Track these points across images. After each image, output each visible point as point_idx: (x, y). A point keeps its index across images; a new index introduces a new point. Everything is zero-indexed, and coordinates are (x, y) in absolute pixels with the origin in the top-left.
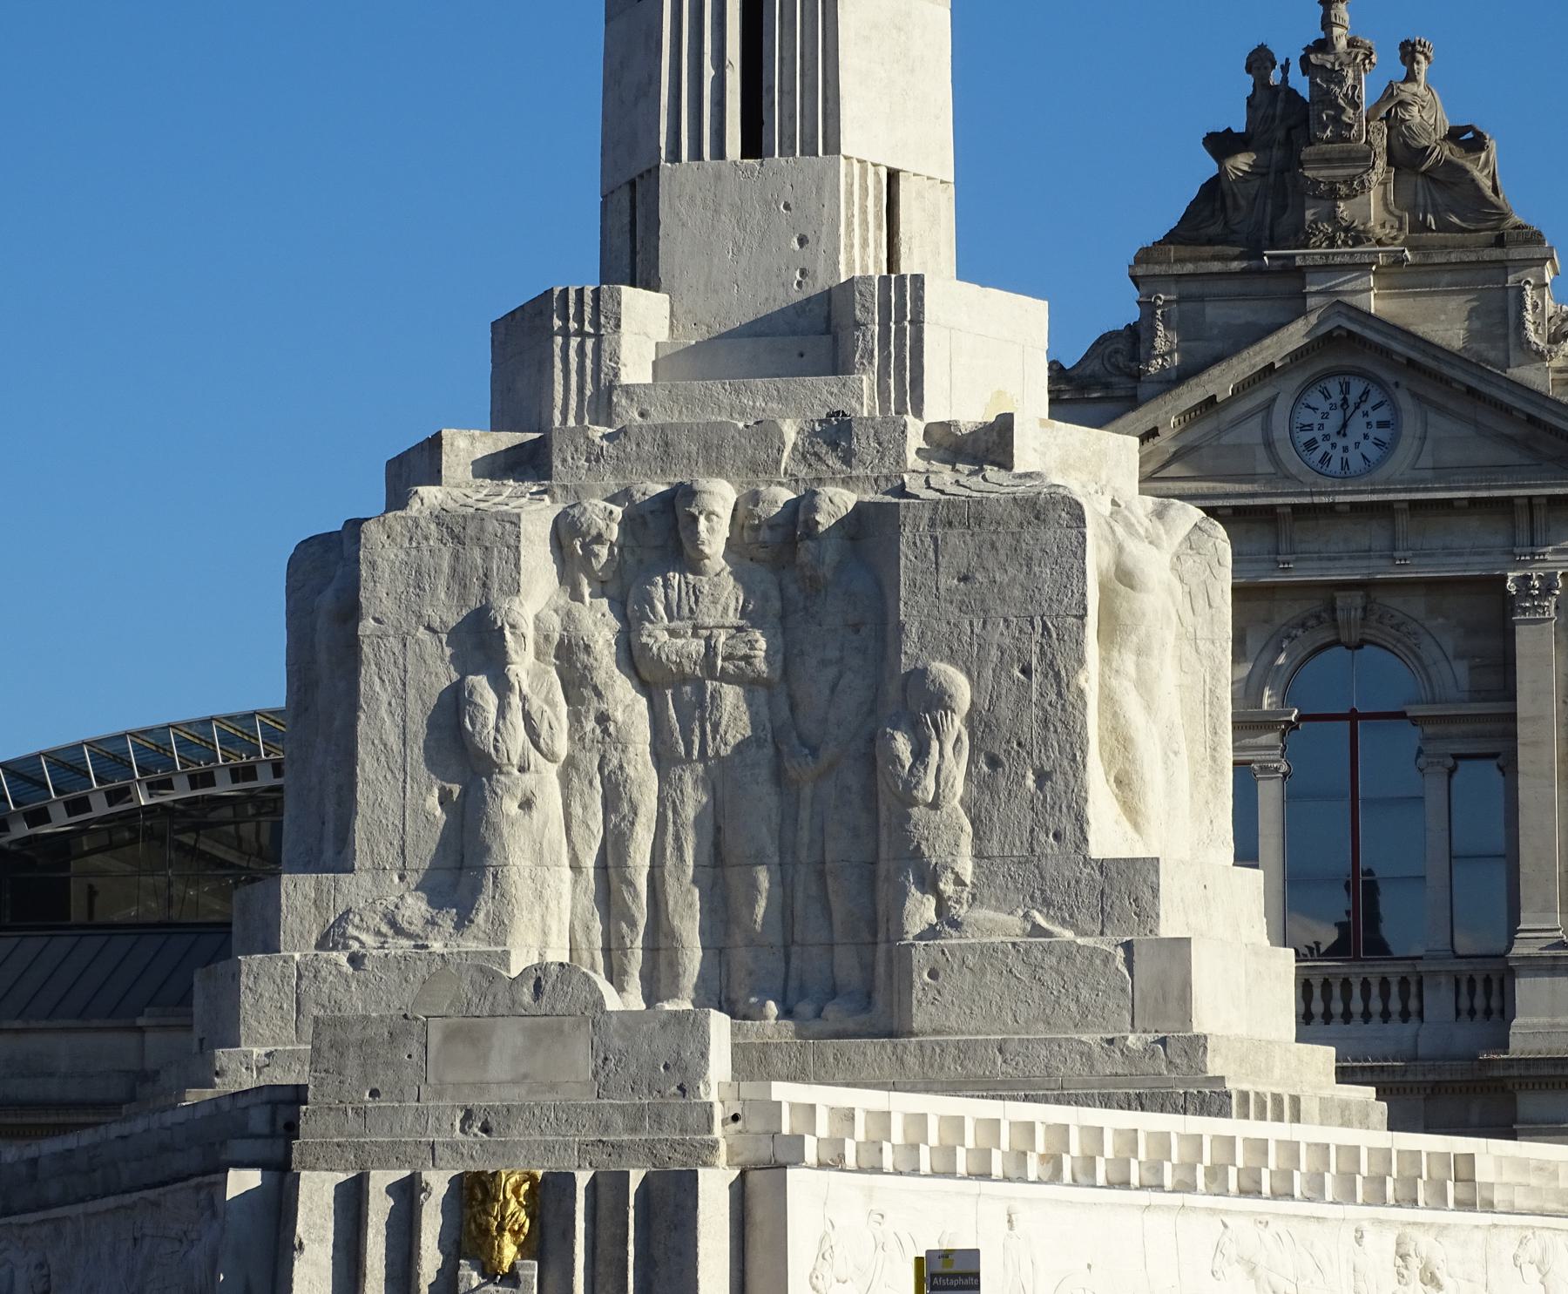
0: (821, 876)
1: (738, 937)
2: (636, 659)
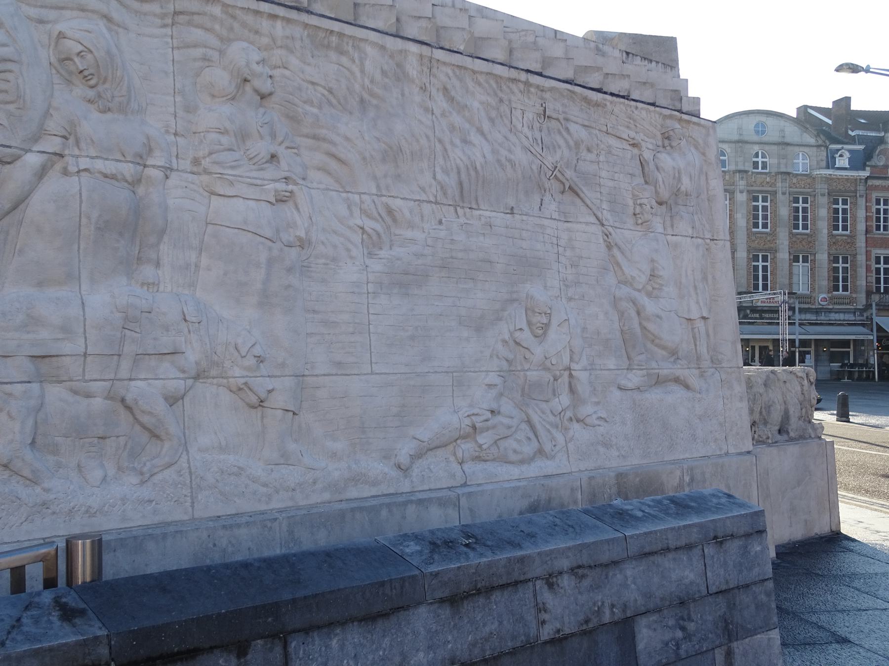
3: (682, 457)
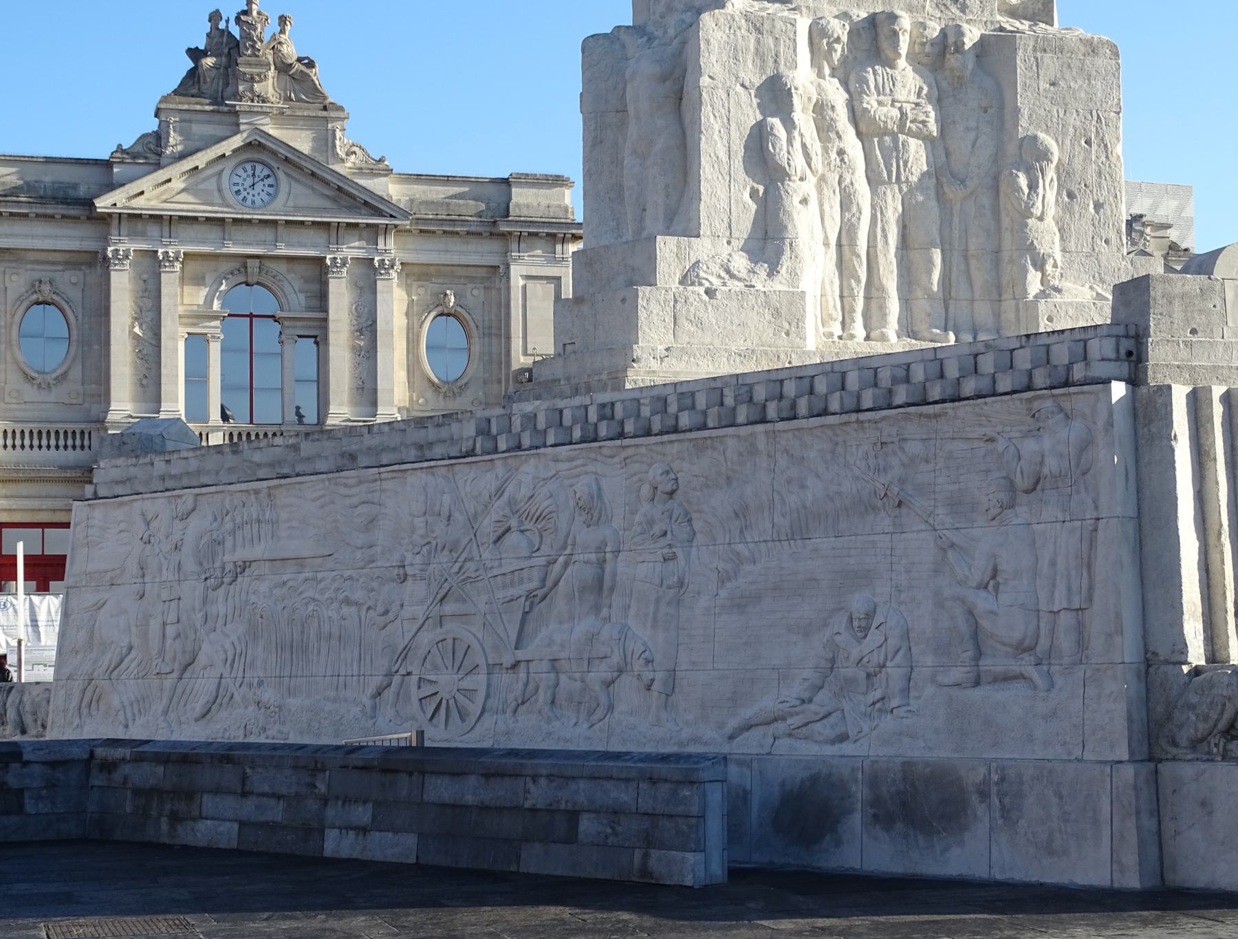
0: (966, 258)
1: (919, 293)
2: (857, 118)
3: (1007, 756)
